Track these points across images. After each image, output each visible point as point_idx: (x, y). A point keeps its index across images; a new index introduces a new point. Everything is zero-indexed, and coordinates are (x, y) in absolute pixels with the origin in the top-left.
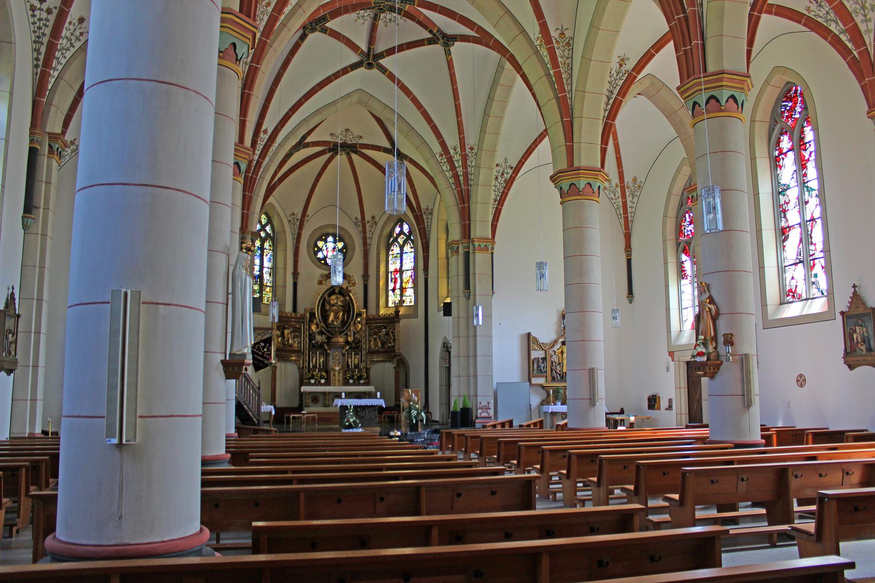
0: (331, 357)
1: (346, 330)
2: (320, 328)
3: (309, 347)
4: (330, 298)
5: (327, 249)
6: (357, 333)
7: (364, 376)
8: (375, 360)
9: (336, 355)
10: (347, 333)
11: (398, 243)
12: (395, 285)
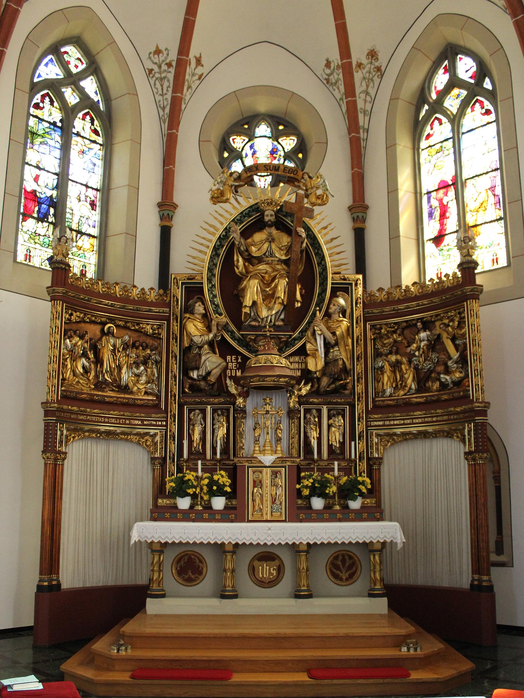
0: (249, 423)
1: (300, 338)
2: (214, 329)
3: (182, 391)
4: (250, 240)
5: (254, 153)
6: (337, 344)
7: (363, 483)
8: (398, 431)
9: (267, 412)
10: (304, 346)
11: (444, 112)
12: (442, 224)
